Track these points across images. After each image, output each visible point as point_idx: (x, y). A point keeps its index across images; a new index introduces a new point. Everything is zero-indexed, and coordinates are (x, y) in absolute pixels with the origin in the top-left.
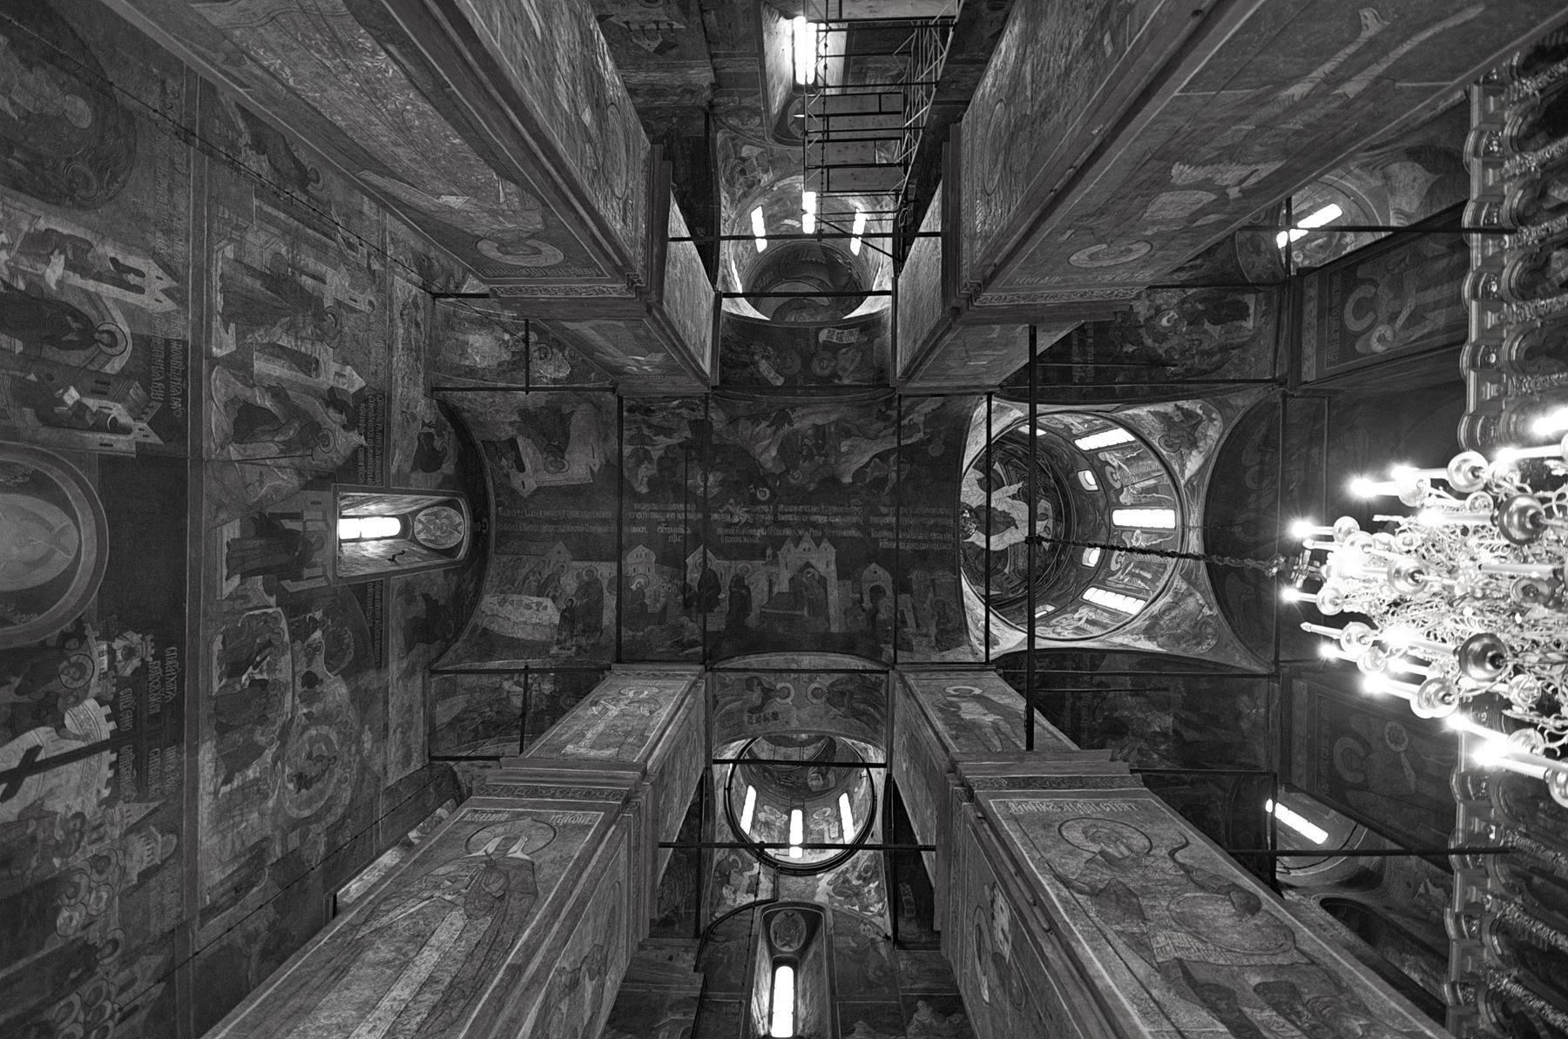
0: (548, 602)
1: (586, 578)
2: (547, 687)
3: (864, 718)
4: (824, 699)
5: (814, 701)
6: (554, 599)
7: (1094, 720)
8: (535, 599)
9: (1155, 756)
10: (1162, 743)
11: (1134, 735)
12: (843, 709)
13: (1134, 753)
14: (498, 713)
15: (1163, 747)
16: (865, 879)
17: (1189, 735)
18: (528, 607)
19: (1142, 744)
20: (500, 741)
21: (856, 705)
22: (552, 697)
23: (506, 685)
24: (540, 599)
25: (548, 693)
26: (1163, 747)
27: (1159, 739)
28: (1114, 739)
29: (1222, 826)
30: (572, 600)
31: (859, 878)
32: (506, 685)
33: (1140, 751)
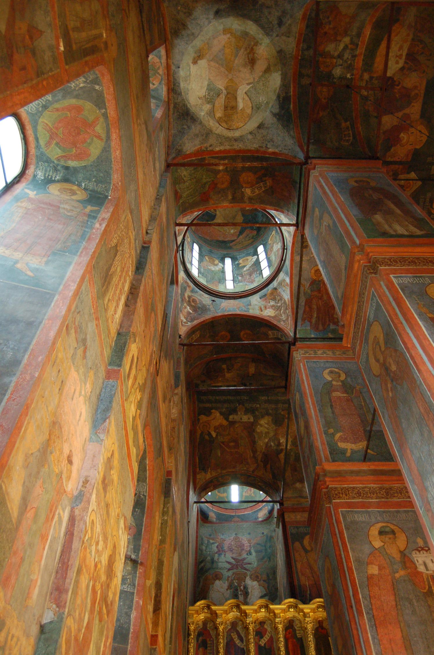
0: (400, 65)
1: (413, 94)
2: (337, 72)
3: (307, 309)
4: (315, 278)
5: (313, 271)
6: (402, 69)
7: (283, 410)
8: (404, 54)
9: (267, 440)
10: (274, 444)
11: (276, 430)
12: (309, 291)
13: (267, 430)
14: (326, 33)
15: (272, 444)
16: (189, 301)
17: (282, 456)
18: (401, 48)
19: (272, 434)
20: (300, 34)
21: (314, 301)
22: (329, 75)
23: (347, 40)
24: (404, 57)
25: (334, 72)
26: (272, 444)
27: (276, 443)
28: (272, 420)
29: (233, 470)
30: (398, 85)
31: (189, 297)
32: (347, 40)
33: (268, 433)
